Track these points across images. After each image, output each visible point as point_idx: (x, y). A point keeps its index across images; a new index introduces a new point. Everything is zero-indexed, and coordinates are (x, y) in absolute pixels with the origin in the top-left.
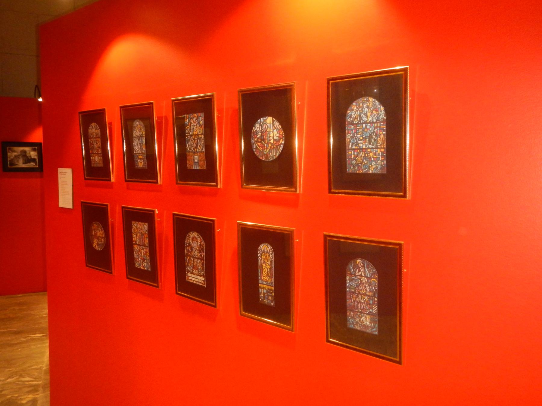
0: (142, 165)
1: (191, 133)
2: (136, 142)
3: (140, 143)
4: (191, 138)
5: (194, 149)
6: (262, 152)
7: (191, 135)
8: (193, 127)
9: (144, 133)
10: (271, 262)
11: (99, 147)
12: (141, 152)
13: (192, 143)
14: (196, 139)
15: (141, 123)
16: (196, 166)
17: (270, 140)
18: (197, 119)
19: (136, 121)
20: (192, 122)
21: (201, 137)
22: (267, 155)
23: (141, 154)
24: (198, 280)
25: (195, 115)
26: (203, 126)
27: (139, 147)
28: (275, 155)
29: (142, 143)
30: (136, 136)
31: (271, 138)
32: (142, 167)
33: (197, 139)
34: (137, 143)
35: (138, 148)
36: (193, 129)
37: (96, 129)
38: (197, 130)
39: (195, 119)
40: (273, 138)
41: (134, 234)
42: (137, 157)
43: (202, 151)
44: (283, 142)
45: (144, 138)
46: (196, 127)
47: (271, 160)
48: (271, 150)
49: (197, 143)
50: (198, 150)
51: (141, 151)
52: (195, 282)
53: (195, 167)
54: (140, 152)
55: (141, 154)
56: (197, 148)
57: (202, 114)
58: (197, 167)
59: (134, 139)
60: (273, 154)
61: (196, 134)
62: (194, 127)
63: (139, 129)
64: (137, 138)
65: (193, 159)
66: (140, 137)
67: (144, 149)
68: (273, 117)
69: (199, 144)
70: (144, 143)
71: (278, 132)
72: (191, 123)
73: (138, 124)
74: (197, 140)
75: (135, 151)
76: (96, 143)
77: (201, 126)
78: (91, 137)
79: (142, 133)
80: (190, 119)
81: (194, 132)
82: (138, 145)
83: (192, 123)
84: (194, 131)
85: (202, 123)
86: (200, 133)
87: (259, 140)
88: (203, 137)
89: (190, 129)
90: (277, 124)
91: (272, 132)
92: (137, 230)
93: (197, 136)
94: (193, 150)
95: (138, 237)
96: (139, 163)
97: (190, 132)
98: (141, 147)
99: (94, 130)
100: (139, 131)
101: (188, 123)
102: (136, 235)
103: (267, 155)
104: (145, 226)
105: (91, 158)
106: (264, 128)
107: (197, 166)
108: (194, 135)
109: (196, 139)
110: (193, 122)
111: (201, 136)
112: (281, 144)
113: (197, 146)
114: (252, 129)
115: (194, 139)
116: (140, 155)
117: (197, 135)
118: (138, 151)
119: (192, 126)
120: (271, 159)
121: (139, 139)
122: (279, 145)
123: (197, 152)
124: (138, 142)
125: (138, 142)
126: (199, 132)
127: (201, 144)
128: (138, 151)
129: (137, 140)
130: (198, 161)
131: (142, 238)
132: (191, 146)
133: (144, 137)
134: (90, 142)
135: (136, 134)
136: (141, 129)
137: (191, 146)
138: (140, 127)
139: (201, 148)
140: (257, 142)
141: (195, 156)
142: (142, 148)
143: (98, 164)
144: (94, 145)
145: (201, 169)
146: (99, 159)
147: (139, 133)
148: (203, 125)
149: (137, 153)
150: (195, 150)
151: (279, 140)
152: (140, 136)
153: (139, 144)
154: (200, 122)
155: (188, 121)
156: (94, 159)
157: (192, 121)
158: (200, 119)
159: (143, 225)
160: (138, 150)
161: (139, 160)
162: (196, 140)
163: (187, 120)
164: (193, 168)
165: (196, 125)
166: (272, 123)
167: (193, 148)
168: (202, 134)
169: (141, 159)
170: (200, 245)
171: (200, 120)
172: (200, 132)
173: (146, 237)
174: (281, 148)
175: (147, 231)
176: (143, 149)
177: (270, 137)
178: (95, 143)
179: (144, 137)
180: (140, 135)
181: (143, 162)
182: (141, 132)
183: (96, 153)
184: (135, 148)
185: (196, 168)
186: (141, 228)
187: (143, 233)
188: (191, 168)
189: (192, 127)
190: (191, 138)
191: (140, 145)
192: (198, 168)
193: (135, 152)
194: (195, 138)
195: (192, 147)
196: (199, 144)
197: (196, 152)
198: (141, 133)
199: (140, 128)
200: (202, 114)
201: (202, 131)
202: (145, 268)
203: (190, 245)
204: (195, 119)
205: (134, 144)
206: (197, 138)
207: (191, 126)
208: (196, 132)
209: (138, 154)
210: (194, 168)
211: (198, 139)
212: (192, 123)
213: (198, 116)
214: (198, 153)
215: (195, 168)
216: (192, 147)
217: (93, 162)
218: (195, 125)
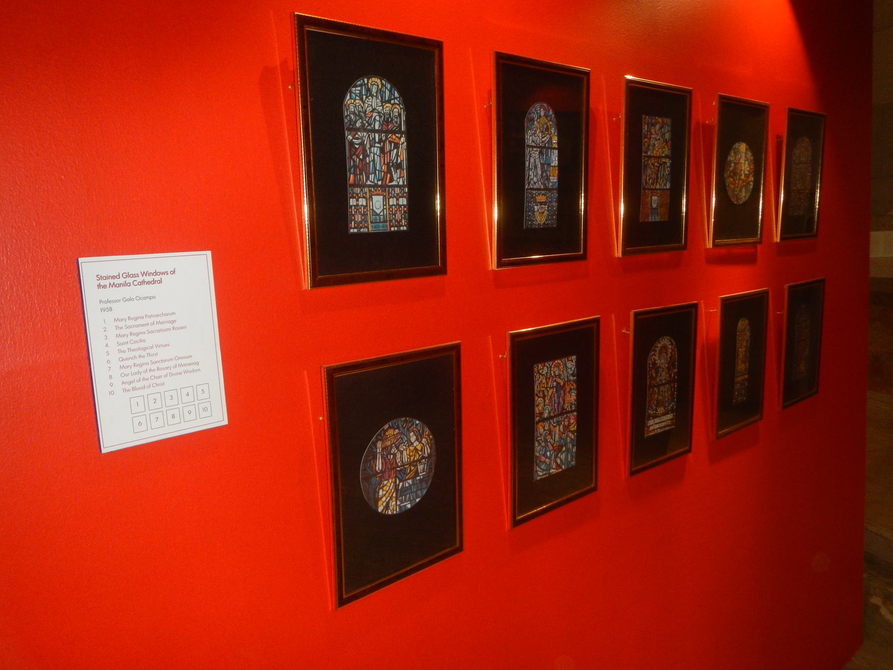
0: (544, 219)
1: (649, 153)
2: (532, 160)
3: (541, 164)
4: (648, 161)
5: (652, 184)
6: (733, 191)
7: (650, 157)
8: (653, 142)
9: (555, 140)
10: (747, 341)
11: (398, 166)
12: (542, 187)
13: (649, 171)
14: (656, 164)
15: (551, 113)
16: (655, 217)
17: (741, 175)
18: (661, 128)
19: (537, 106)
20: (653, 133)
21: (665, 163)
22: (737, 195)
23: (542, 190)
24: (663, 424)
25: (660, 120)
26: (669, 143)
27: (540, 172)
28: (745, 197)
29: (549, 165)
30: (533, 144)
31: (742, 172)
32: (544, 223)
33: (658, 165)
34: (535, 162)
35: (536, 176)
36: (654, 145)
37: (389, 101)
38: (659, 149)
39: (658, 127)
40: (744, 172)
41: (539, 397)
42: (533, 197)
43: (665, 187)
44: (752, 179)
45: (556, 152)
46: (658, 141)
47: (741, 203)
48: (741, 191)
49: (658, 173)
50: (658, 187)
51: (545, 185)
52: (659, 431)
53: (653, 217)
54: (539, 185)
55: (543, 192)
56: (657, 183)
57: (669, 121)
58: (656, 217)
59: (527, 151)
60: (744, 194)
61: (658, 155)
62: (656, 143)
63: (543, 126)
64: (534, 149)
65: (650, 202)
66: (543, 149)
67: (554, 179)
68: (747, 144)
69: (661, 174)
70: (553, 164)
71: (749, 164)
72: (651, 134)
73: (542, 114)
74: (659, 167)
75: (529, 183)
76: (382, 150)
77: (666, 142)
78: (358, 125)
79: (551, 138)
80: (650, 125)
81: (655, 152)
82: (536, 167)
83: (653, 134)
84: (654, 149)
85: (668, 136)
86: (663, 155)
87: (732, 174)
88: (668, 162)
89: (649, 146)
90: (749, 154)
91: (743, 164)
92: (547, 384)
93: (658, 160)
94: (650, 186)
95: (547, 401)
96: (537, 214)
97: (649, 150)
98: (544, 175)
99: (375, 102)
100: (542, 132)
101: (646, 133)
102: (544, 397)
103: (737, 195)
104: (569, 365)
105: (352, 202)
106: (737, 157)
107: (656, 215)
108: (653, 157)
109: (656, 164)
110: (655, 132)
111: (664, 160)
112: (751, 181)
113: (657, 178)
114: (727, 158)
115: (653, 165)
116: (539, 194)
117: (660, 157)
118: (535, 183)
119: (652, 139)
120: (741, 201)
121: (541, 153)
122: (748, 183)
123: (657, 189)
124: (537, 160)
125: (537, 160)
126: (663, 153)
127: (663, 175)
128: (535, 183)
129: (535, 154)
130: (658, 205)
131: (559, 398)
132: (648, 178)
133: (555, 148)
134: (352, 144)
135: (535, 139)
136: (547, 129)
137: (648, 178)
138: (546, 124)
139: (663, 181)
140: (730, 176)
141: (653, 197)
142: (547, 175)
143: (385, 221)
144: (366, 156)
145: (662, 220)
146: (391, 206)
147: (543, 138)
148: (669, 140)
149: (533, 189)
150: (653, 186)
151: (749, 175)
152: (545, 147)
153: (539, 166)
154: (665, 133)
155: (646, 130)
156: (365, 207)
157: (653, 131)
158: (667, 129)
159: (565, 365)
160: (535, 179)
161: (536, 207)
162: (657, 166)
163: (646, 126)
164: (650, 220)
165: (659, 139)
166: (744, 151)
167: (651, 180)
168: (666, 157)
169: (541, 203)
170: (671, 357)
171: (666, 131)
172: (663, 153)
173: (571, 389)
174: (751, 187)
175: (573, 375)
176: (548, 179)
177: (741, 170)
178: (376, 150)
179: (555, 148)
180: (543, 142)
181: (548, 211)
182: (548, 136)
183: (376, 186)
184: (529, 176)
185: (655, 219)
186: (557, 373)
187: (562, 384)
188: (646, 220)
189: (652, 142)
190: (649, 162)
191: (542, 168)
192: (658, 219)
193: (529, 185)
194: (655, 163)
195: (649, 180)
196: (661, 174)
197: (656, 189)
198: (546, 139)
199: (545, 126)
200: (669, 121)
201: (667, 152)
202: (561, 468)
203: (654, 364)
204: (658, 127)
205: (527, 163)
206: (658, 163)
207: (651, 138)
208: (657, 151)
209: (534, 192)
210: (652, 219)
211: (661, 165)
212: (653, 134)
213: (663, 122)
214: (658, 191)
215: (653, 220)
216: (649, 180)
217: (358, 218)
218: (658, 138)
